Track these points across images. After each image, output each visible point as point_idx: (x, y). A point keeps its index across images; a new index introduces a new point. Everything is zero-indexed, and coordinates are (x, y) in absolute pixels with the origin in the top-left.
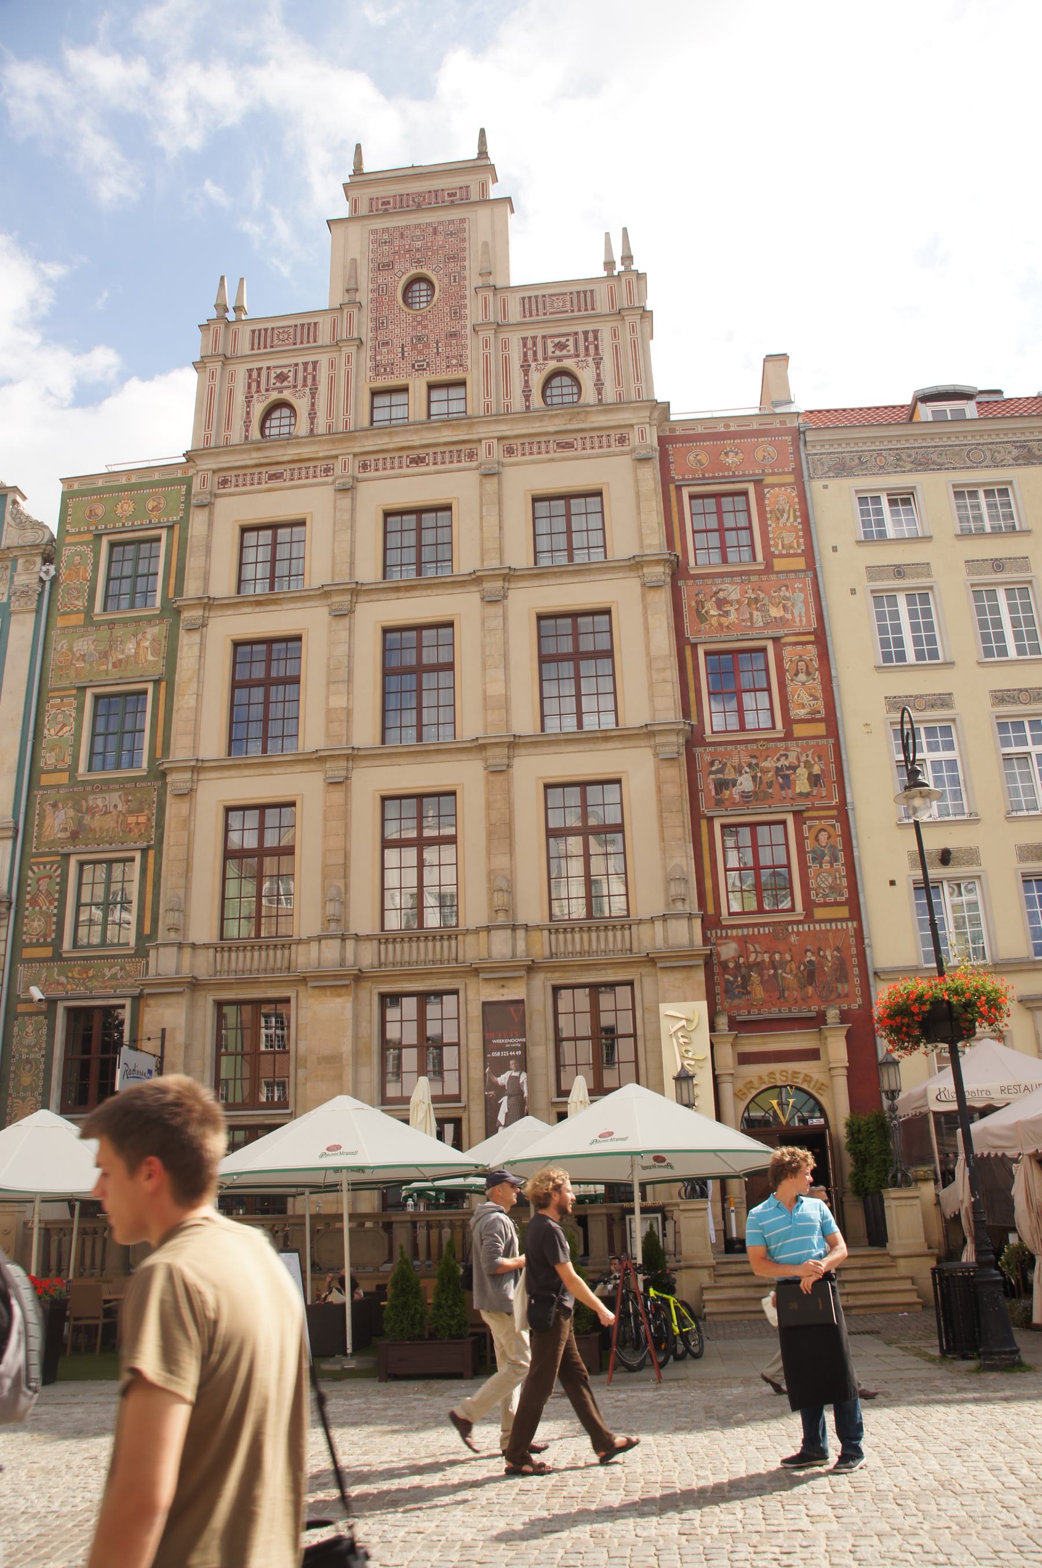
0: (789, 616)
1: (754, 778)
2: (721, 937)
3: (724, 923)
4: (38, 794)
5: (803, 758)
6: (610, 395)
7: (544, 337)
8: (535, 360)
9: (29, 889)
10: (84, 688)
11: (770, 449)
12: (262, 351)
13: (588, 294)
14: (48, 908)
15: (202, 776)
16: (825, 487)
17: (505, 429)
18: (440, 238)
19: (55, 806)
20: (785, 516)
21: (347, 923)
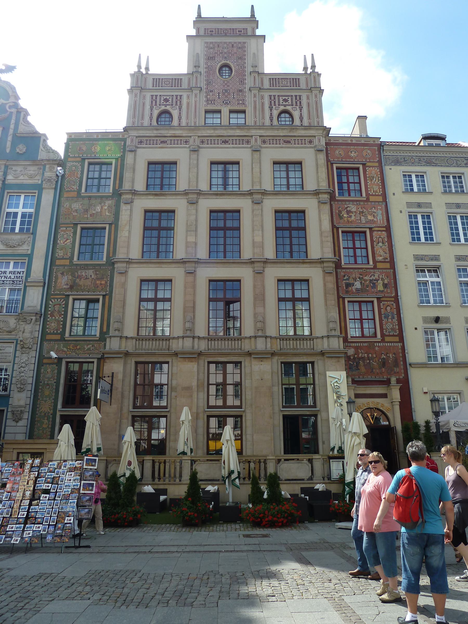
1: (361, 283)
2: (348, 346)
3: (349, 341)
4: (55, 268)
5: (381, 277)
6: (306, 123)
7: (278, 96)
8: (275, 105)
9: (50, 309)
10: (77, 224)
11: (369, 151)
12: (157, 88)
13: (297, 80)
14: (59, 318)
15: (131, 266)
16: (390, 169)
17: (262, 132)
18: (235, 49)
19: (62, 274)
20: (375, 179)
21: (194, 331)
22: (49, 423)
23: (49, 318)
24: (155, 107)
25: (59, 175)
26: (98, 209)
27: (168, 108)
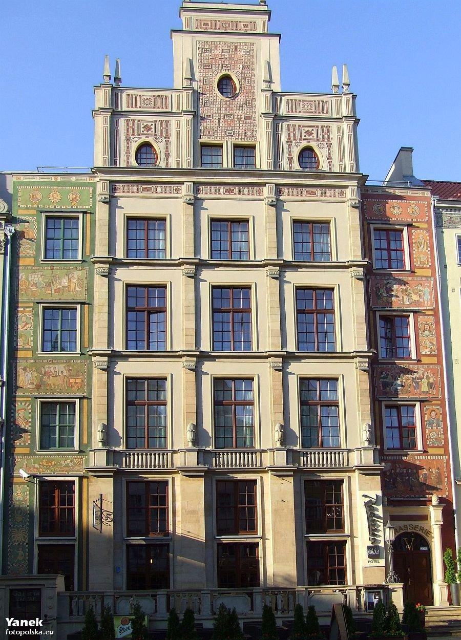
0: (421, 300)
8: (295, 139)
11: (416, 208)
13: (324, 103)
14: (25, 426)
18: (239, 53)
19: (25, 369)
20: (422, 246)
22: (25, 554)
23: (12, 426)
24: (132, 137)
26: (65, 282)
27: (151, 139)
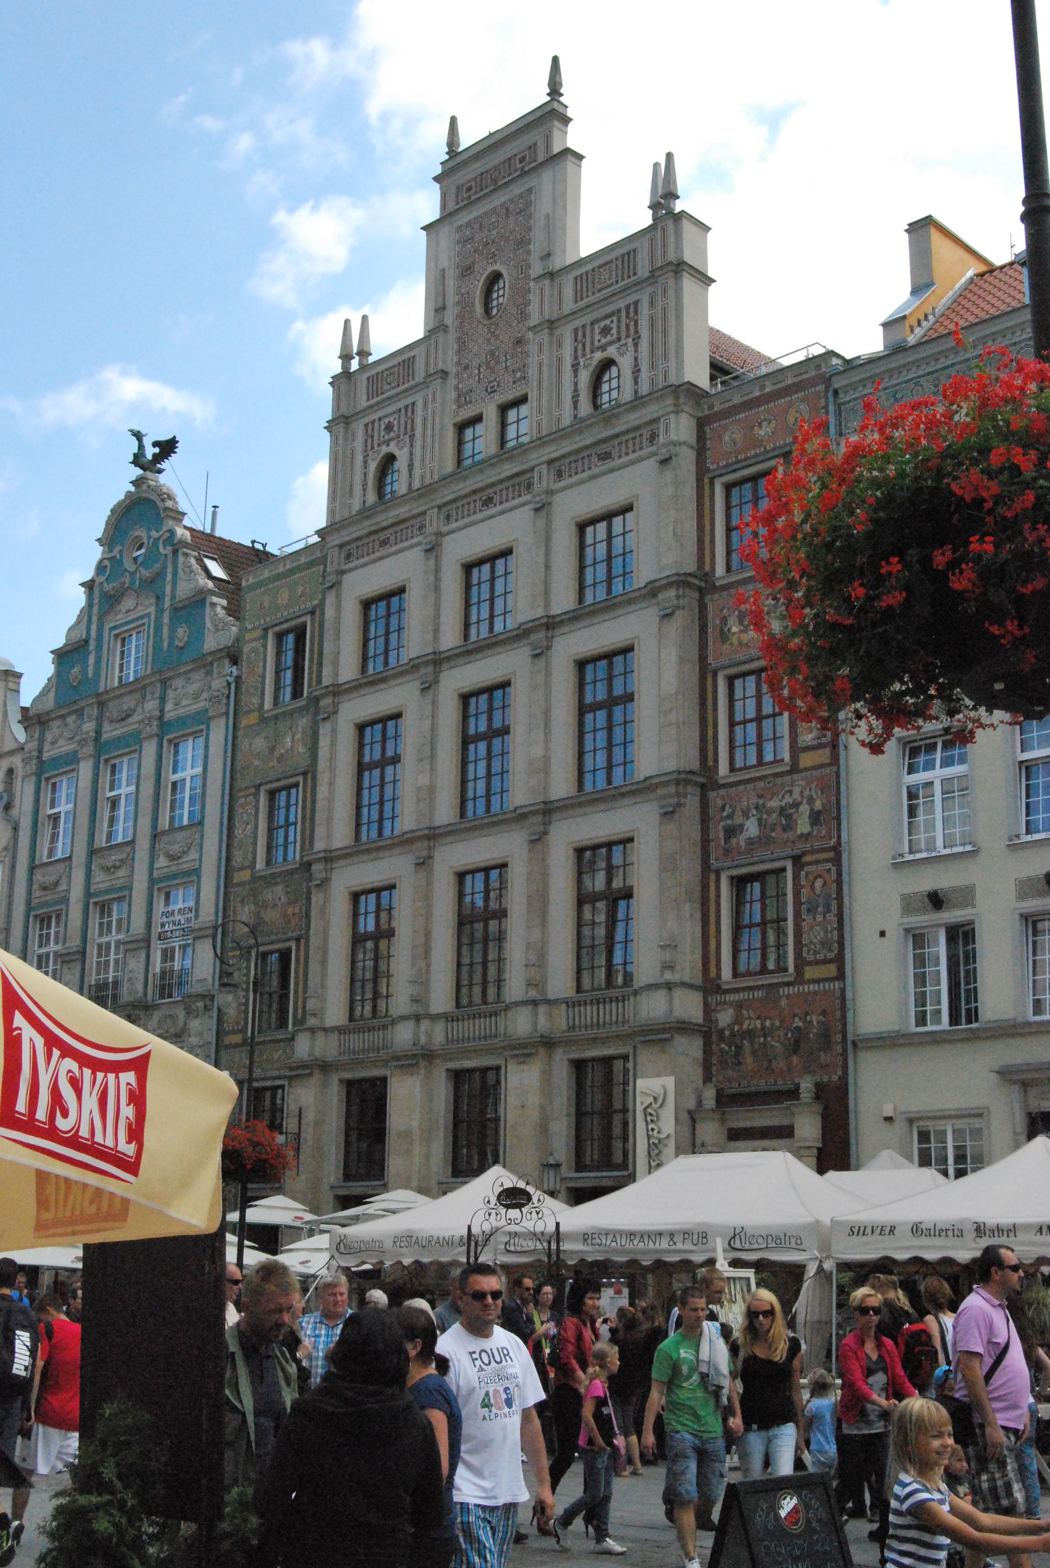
1: (760, 820)
11: (803, 407)
19: (242, 902)
25: (231, 680)
